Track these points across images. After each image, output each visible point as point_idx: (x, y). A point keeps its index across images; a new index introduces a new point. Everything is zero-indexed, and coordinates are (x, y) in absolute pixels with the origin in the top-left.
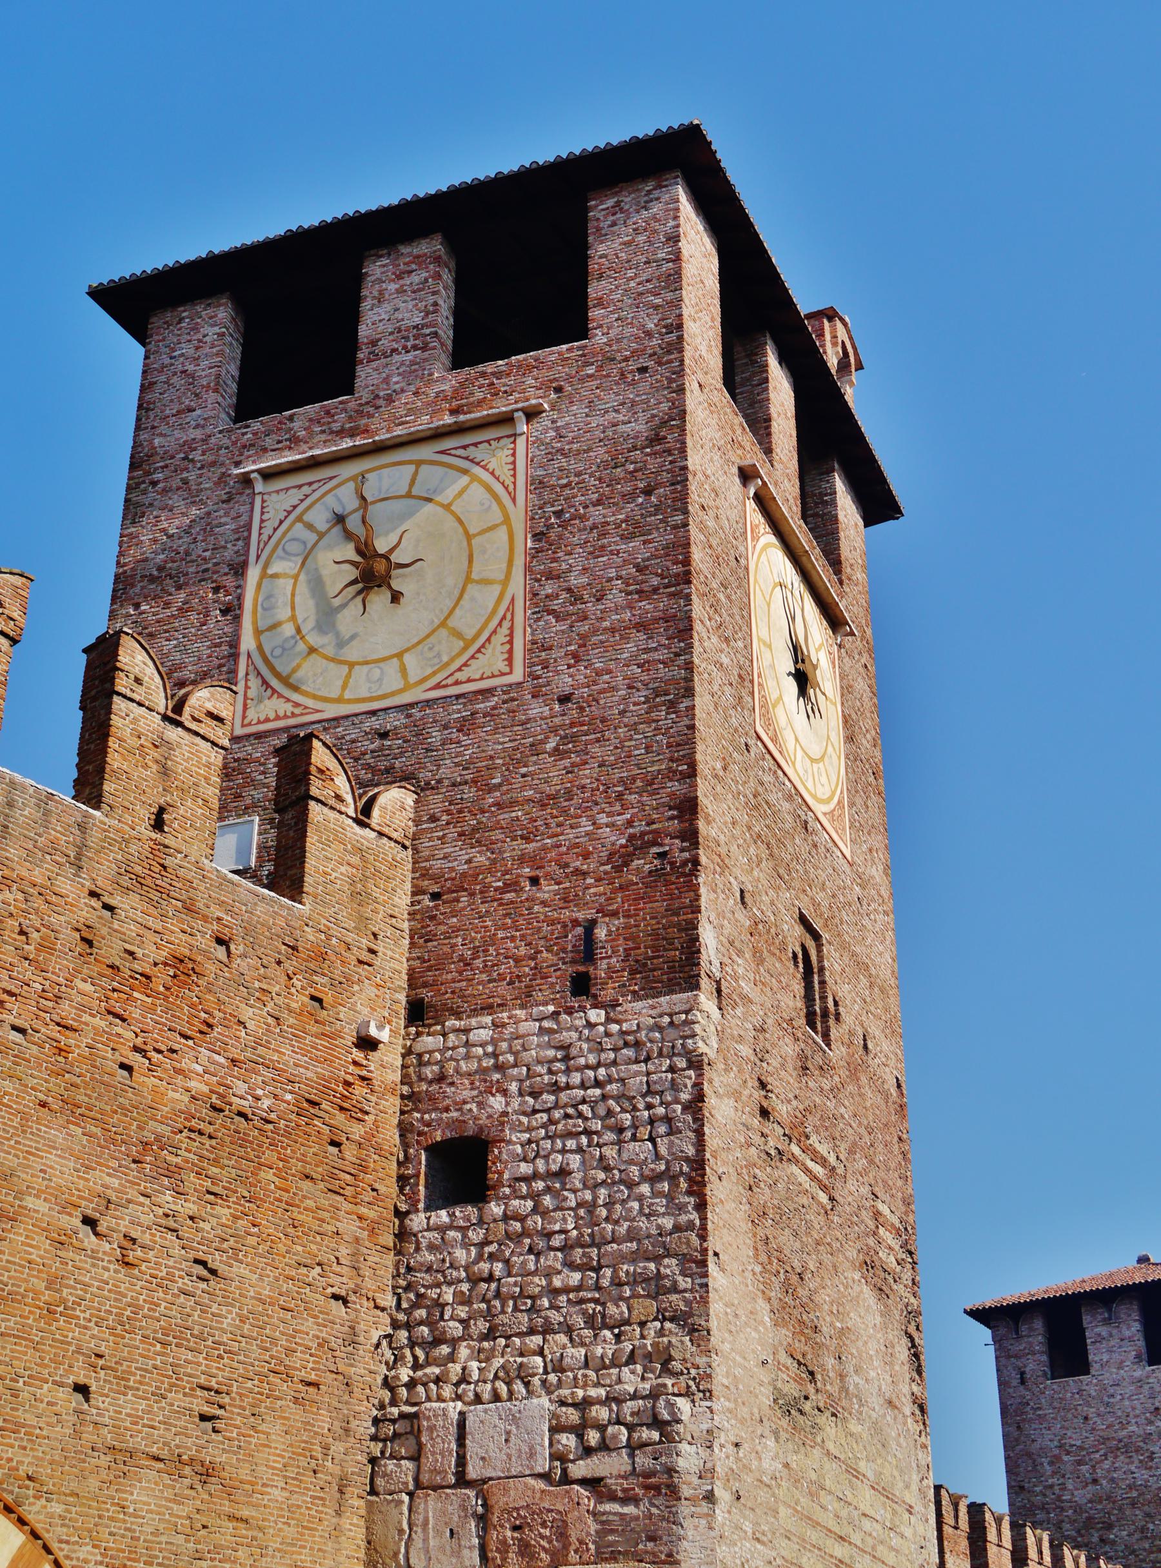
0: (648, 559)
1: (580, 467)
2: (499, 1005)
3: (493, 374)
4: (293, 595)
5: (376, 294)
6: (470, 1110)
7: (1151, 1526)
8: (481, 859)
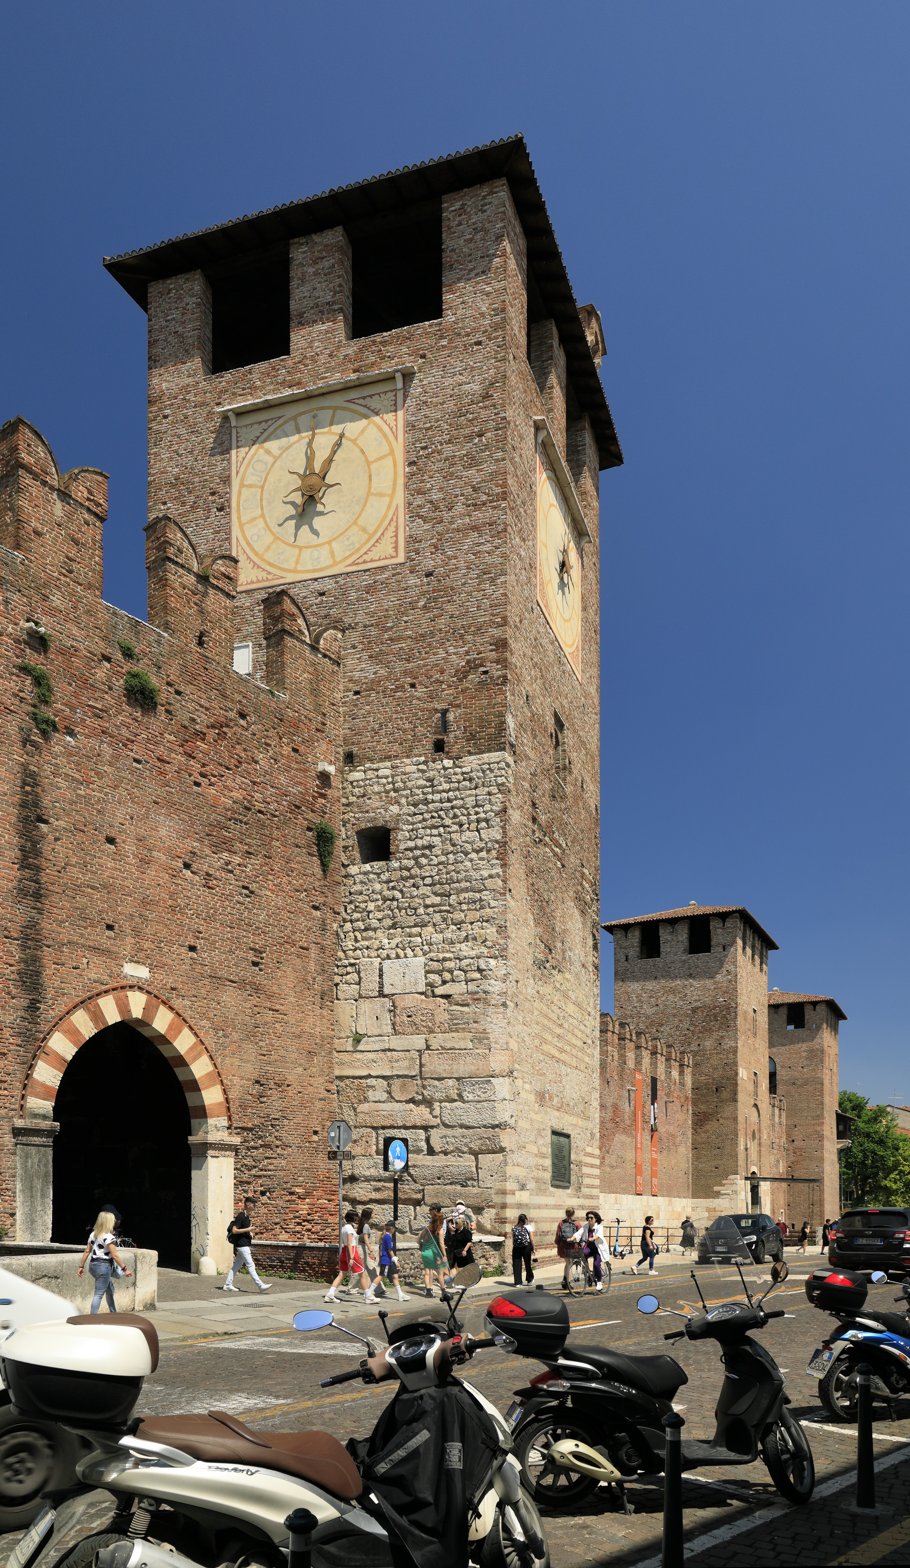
0: (480, 482)
1: (439, 415)
2: (395, 756)
3: (381, 343)
4: (261, 500)
5: (300, 275)
6: (380, 813)
8: (383, 672)
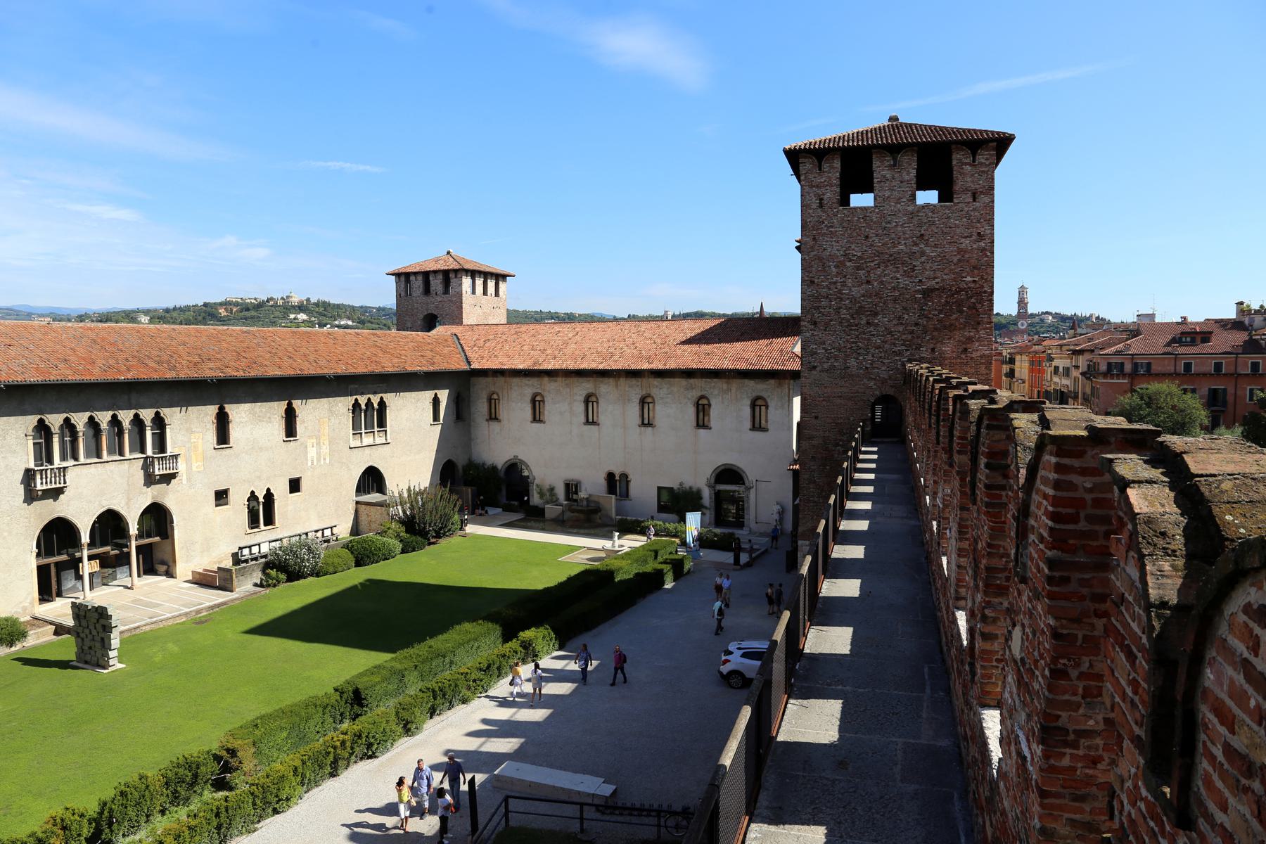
7: (906, 317)
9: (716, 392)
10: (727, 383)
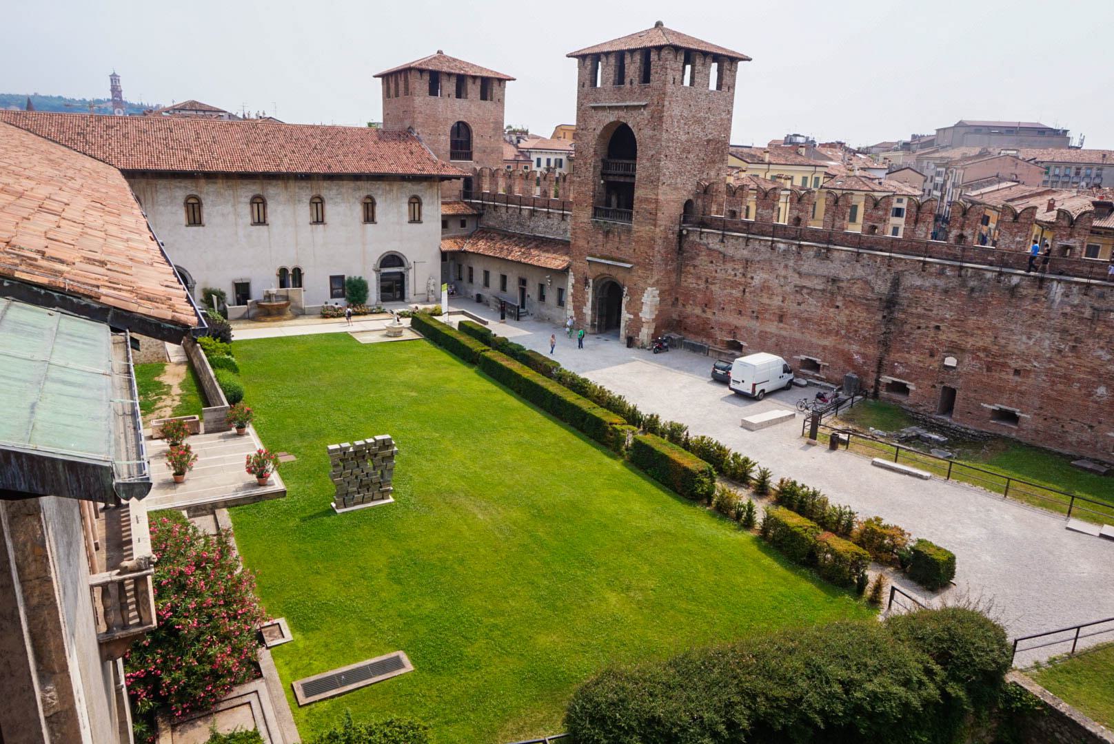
9: (380, 192)
10: (389, 184)
